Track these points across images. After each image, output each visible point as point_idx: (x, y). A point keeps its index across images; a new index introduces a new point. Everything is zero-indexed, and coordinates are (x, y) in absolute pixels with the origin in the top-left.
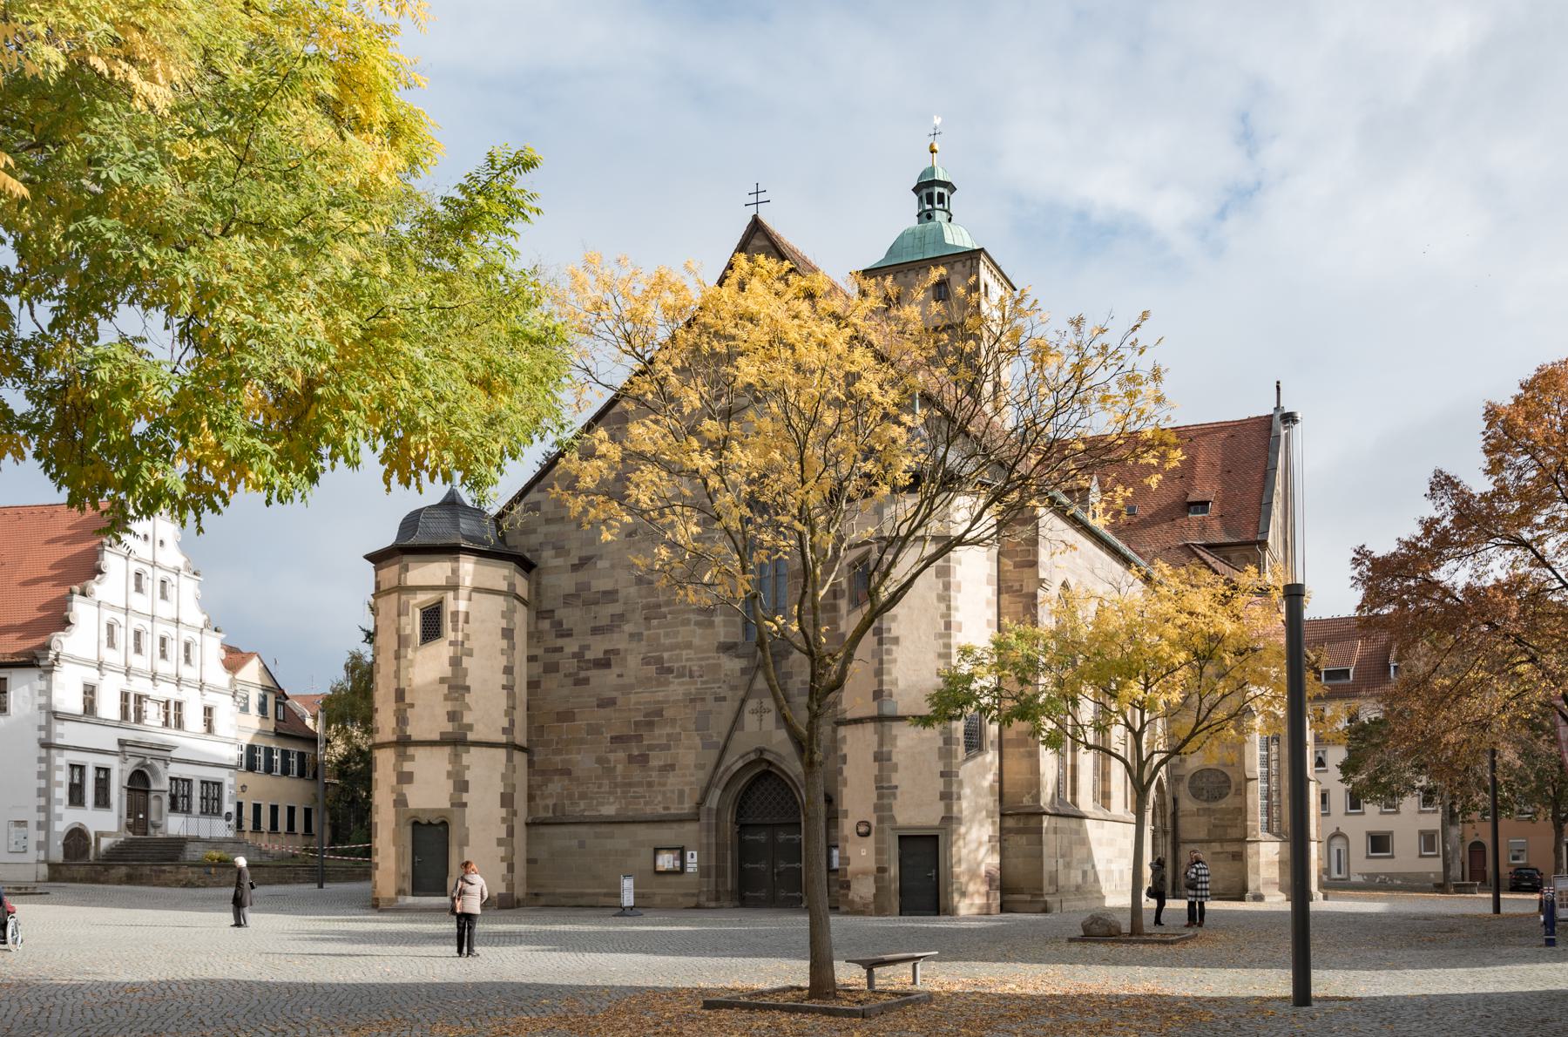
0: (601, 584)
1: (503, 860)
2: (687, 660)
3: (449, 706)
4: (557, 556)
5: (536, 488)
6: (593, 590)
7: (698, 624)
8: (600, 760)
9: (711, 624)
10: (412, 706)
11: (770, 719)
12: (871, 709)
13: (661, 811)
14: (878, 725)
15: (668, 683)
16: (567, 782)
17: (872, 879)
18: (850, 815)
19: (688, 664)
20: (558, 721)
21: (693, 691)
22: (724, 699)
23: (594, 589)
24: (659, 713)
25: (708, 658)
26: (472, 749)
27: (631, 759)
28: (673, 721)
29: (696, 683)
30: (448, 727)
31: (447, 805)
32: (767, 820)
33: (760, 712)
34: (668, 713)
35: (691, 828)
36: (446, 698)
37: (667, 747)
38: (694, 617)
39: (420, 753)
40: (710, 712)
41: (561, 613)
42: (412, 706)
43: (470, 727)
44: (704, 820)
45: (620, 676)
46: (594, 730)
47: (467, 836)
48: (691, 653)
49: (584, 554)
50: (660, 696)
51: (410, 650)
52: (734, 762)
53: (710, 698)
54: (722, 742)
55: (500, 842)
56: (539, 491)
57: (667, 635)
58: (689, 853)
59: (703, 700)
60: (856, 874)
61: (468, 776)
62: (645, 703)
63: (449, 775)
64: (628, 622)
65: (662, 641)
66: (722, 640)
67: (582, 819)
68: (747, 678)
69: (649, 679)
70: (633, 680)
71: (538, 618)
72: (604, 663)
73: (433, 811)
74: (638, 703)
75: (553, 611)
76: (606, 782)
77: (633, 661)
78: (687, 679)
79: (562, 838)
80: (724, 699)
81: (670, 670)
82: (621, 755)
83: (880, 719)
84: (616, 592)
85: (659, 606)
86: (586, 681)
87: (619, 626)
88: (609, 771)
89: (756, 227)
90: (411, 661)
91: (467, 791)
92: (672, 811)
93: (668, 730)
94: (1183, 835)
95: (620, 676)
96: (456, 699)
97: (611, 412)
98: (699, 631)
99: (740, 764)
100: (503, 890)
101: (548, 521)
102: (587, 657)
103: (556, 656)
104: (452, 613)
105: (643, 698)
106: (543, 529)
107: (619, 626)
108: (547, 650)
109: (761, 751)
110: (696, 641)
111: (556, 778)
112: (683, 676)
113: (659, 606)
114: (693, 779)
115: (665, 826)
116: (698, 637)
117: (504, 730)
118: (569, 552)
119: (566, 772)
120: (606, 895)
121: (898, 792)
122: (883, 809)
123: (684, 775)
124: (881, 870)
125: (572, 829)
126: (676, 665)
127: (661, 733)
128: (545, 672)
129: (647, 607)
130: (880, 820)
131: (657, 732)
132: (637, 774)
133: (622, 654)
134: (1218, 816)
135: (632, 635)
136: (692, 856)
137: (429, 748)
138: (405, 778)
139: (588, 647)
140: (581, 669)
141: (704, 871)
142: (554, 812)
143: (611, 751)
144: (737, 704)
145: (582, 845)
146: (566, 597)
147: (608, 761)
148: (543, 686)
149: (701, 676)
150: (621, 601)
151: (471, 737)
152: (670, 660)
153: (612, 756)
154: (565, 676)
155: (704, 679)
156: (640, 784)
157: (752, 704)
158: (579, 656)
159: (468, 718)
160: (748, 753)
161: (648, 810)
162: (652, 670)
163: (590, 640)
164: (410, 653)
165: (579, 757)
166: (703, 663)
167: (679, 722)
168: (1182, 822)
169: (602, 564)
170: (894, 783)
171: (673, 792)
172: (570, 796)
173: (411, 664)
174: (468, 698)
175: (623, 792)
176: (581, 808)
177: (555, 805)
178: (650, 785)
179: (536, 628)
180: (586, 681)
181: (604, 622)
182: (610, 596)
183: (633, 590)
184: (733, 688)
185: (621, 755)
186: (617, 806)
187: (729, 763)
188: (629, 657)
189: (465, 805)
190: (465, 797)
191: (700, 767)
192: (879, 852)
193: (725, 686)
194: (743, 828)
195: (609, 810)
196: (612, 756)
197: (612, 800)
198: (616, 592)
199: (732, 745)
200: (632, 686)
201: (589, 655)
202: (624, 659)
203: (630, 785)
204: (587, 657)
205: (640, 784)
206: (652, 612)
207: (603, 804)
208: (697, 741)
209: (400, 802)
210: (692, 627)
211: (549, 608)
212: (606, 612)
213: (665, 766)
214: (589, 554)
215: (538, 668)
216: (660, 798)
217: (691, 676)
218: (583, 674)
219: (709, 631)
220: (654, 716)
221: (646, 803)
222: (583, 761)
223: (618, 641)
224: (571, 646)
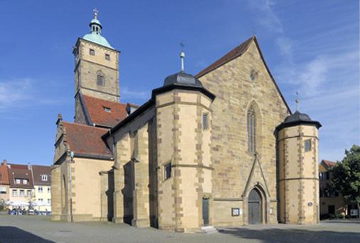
9: (244, 145)
11: (260, 174)
13: (232, 197)
15: (233, 159)
27: (224, 180)
33: (257, 172)
34: (234, 168)
37: (233, 178)
50: (232, 162)
52: (252, 185)
54: (247, 179)
77: (225, 151)
81: (234, 156)
105: (228, 162)
116: (241, 147)
127: (232, 174)
129: (228, 135)
132: (226, 186)
141: (244, 215)
144: (250, 169)
157: (255, 170)
162: (230, 154)
178: (229, 189)
181: (216, 136)
183: (225, 129)
191: (242, 185)
208: (241, 178)
209: (199, 190)
220: (230, 169)
223: (220, 143)
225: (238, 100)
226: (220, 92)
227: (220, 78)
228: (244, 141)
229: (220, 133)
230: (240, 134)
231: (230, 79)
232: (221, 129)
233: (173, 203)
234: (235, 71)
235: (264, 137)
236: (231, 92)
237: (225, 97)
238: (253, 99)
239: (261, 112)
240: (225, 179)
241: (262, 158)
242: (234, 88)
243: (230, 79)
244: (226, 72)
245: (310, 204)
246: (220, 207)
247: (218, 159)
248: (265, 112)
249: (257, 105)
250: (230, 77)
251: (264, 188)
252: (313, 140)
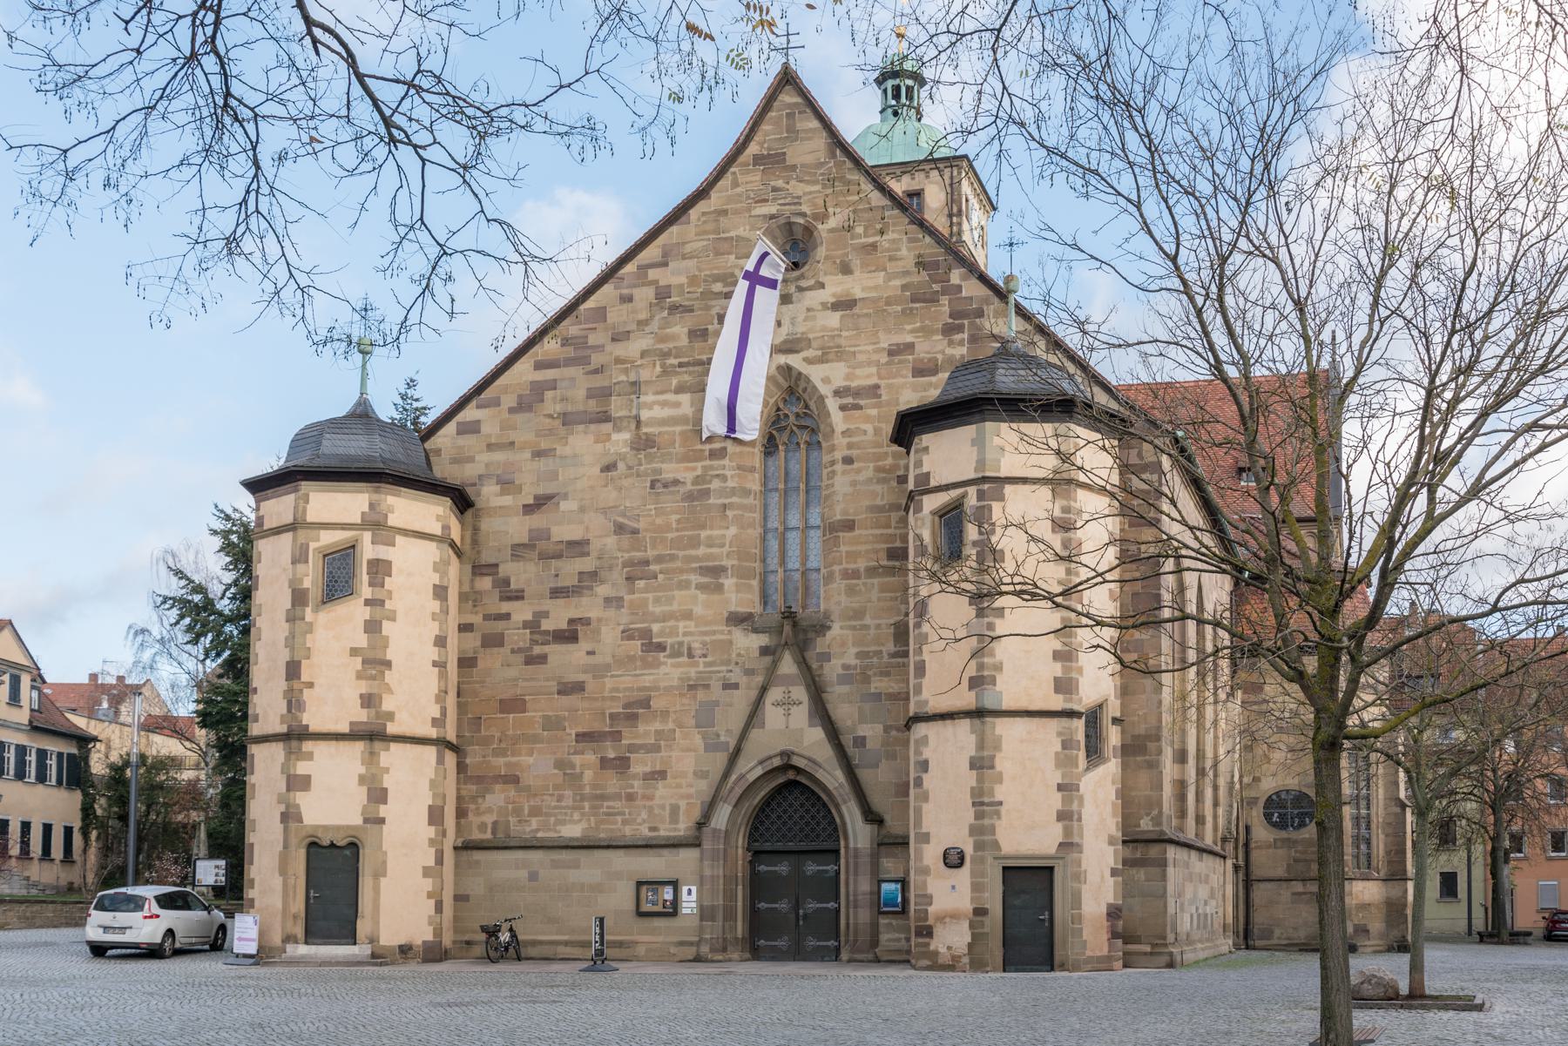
0: (565, 532)
1: (430, 895)
2: (685, 634)
3: (364, 687)
4: (503, 493)
5: (474, 403)
6: (555, 539)
7: (700, 587)
8: (560, 764)
9: (719, 588)
10: (311, 685)
11: (801, 714)
12: (966, 699)
13: (645, 831)
14: (977, 721)
15: (658, 665)
16: (513, 793)
17: (966, 924)
18: (933, 840)
19: (686, 639)
20: (502, 712)
21: (693, 675)
22: (736, 686)
23: (555, 539)
24: (645, 703)
25: (714, 633)
26: (393, 746)
27: (604, 763)
28: (665, 714)
29: (696, 664)
30: (362, 716)
31: (359, 821)
32: (791, 846)
33: (787, 704)
35: (690, 855)
36: (359, 676)
37: (656, 748)
38: (695, 578)
39: (319, 749)
40: (716, 703)
41: (508, 569)
42: (311, 685)
43: (390, 716)
44: (707, 845)
45: (589, 653)
46: (552, 724)
47: (384, 862)
48: (691, 625)
49: (541, 491)
50: (647, 680)
51: (308, 610)
52: (750, 768)
53: (716, 686)
54: (732, 744)
55: (427, 872)
56: (478, 407)
57: (657, 601)
58: (685, 889)
59: (707, 687)
60: (941, 919)
61: (387, 781)
62: (626, 689)
63: (362, 780)
64: (602, 582)
65: (651, 608)
66: (733, 608)
67: (535, 843)
68: (768, 659)
69: (632, 659)
70: (609, 659)
71: (474, 574)
72: (568, 636)
73: (338, 828)
74: (616, 690)
75: (496, 565)
76: (568, 793)
77: (609, 638)
78: (684, 659)
79: (505, 867)
80: (736, 686)
81: (661, 647)
82: (591, 758)
83: (979, 713)
84: (587, 542)
85: (647, 563)
86: (542, 659)
87: (591, 588)
88: (573, 779)
89: (787, 79)
90: (311, 624)
91: (385, 802)
92: (662, 833)
93: (657, 726)
94: (1257, 872)
95: (589, 653)
96: (373, 678)
97: (582, 307)
98: (702, 597)
99: (759, 771)
100: (430, 937)
101: (490, 447)
102: (543, 628)
103: (500, 626)
104: (370, 562)
105: (623, 683)
106: (485, 457)
107: (591, 588)
108: (487, 617)
109: (786, 754)
110: (698, 610)
111: (498, 787)
112: (679, 654)
113: (647, 563)
114: (692, 790)
115: (651, 851)
116: (701, 604)
117: (435, 722)
118: (519, 489)
119: (512, 780)
120: (566, 943)
121: (1003, 809)
122: (982, 832)
123: (679, 786)
124: (980, 912)
125: (520, 854)
126: (670, 641)
127: (647, 730)
128: (483, 646)
129: (629, 563)
130: (979, 846)
131: (641, 728)
132: (612, 783)
133: (594, 624)
134: (1300, 848)
135: (608, 600)
136: (690, 892)
137: (334, 742)
138: (297, 783)
139: (546, 614)
140: (534, 642)
142: (494, 833)
143: (575, 753)
144: (754, 694)
145: (533, 876)
146: (515, 547)
147: (573, 767)
148: (481, 664)
149: (705, 656)
150: (594, 554)
151: (391, 729)
152: (662, 633)
153: (577, 759)
154: (513, 651)
155: (709, 659)
156: (617, 797)
157: (775, 694)
158: (533, 625)
159: (388, 704)
160: (770, 758)
161: (628, 831)
163: (548, 605)
164: (309, 614)
165: (531, 760)
166: (707, 639)
167: (672, 715)
168: (1254, 855)
169: (564, 506)
170: (998, 798)
171: (663, 807)
172: (517, 811)
173: (310, 628)
174: (389, 677)
175: (592, 807)
176: (533, 827)
177: (495, 823)
178: (631, 797)
179: (472, 588)
180: (542, 659)
181: (569, 581)
182: (578, 547)
183: (611, 541)
184: (749, 672)
185: (591, 758)
186: (584, 825)
187: (743, 771)
188: (604, 629)
189: (382, 821)
190: (383, 811)
192: (976, 888)
193: (737, 670)
194: (757, 855)
195: (573, 831)
196: (577, 760)
197: (576, 816)
198: (587, 542)
199: (748, 746)
200: (608, 667)
201: (547, 625)
202: (598, 631)
203: (603, 797)
204: (543, 628)
205: (617, 797)
206: (637, 571)
207: (563, 823)
208: (698, 741)
209: (290, 816)
210: (693, 591)
211: (492, 561)
212: (571, 569)
213: (653, 773)
214: (549, 491)
215: (473, 641)
216: (644, 815)
217: (690, 655)
218: (537, 650)
219: (716, 597)
220: (637, 708)
221: (625, 822)
222: (536, 765)
223: (588, 606)
224: (521, 612)
225: (685, 398)
226: (591, 394)
227: (593, 339)
228: (717, 571)
229: (587, 564)
230: (695, 543)
231: (642, 324)
232: (594, 547)
234: (673, 276)
235: (849, 526)
236: (645, 375)
237: (617, 407)
239: (832, 404)
240: (612, 755)
241: (836, 630)
242: (665, 355)
243: (642, 324)
244: (630, 299)
245: (953, 859)
246: (573, 876)
247: (574, 677)
248: (852, 397)
249: (808, 380)
250: (643, 316)
251: (833, 778)
252: (972, 500)
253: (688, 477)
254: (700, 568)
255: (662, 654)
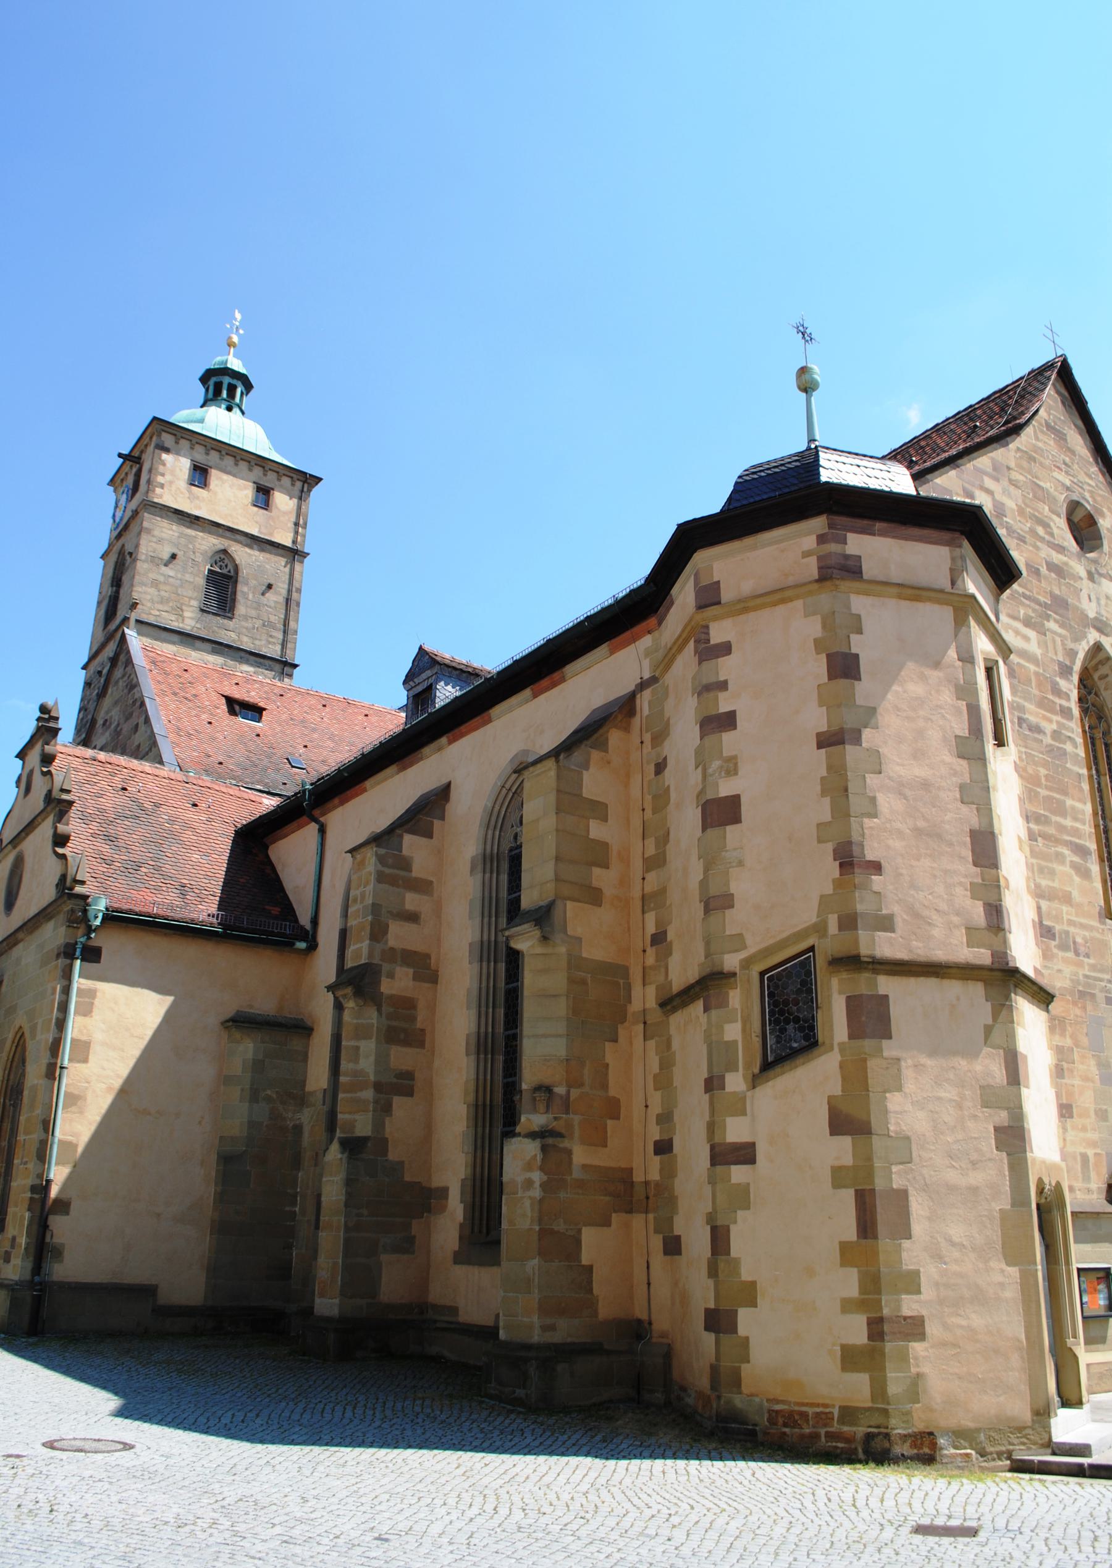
126: (1058, 928)
210: (1067, 869)
219: (1086, 883)
225: (1032, 634)
233: (850, 1233)
238: (1093, 636)
253: (1049, 728)
254: (1071, 842)
255: (1053, 943)
